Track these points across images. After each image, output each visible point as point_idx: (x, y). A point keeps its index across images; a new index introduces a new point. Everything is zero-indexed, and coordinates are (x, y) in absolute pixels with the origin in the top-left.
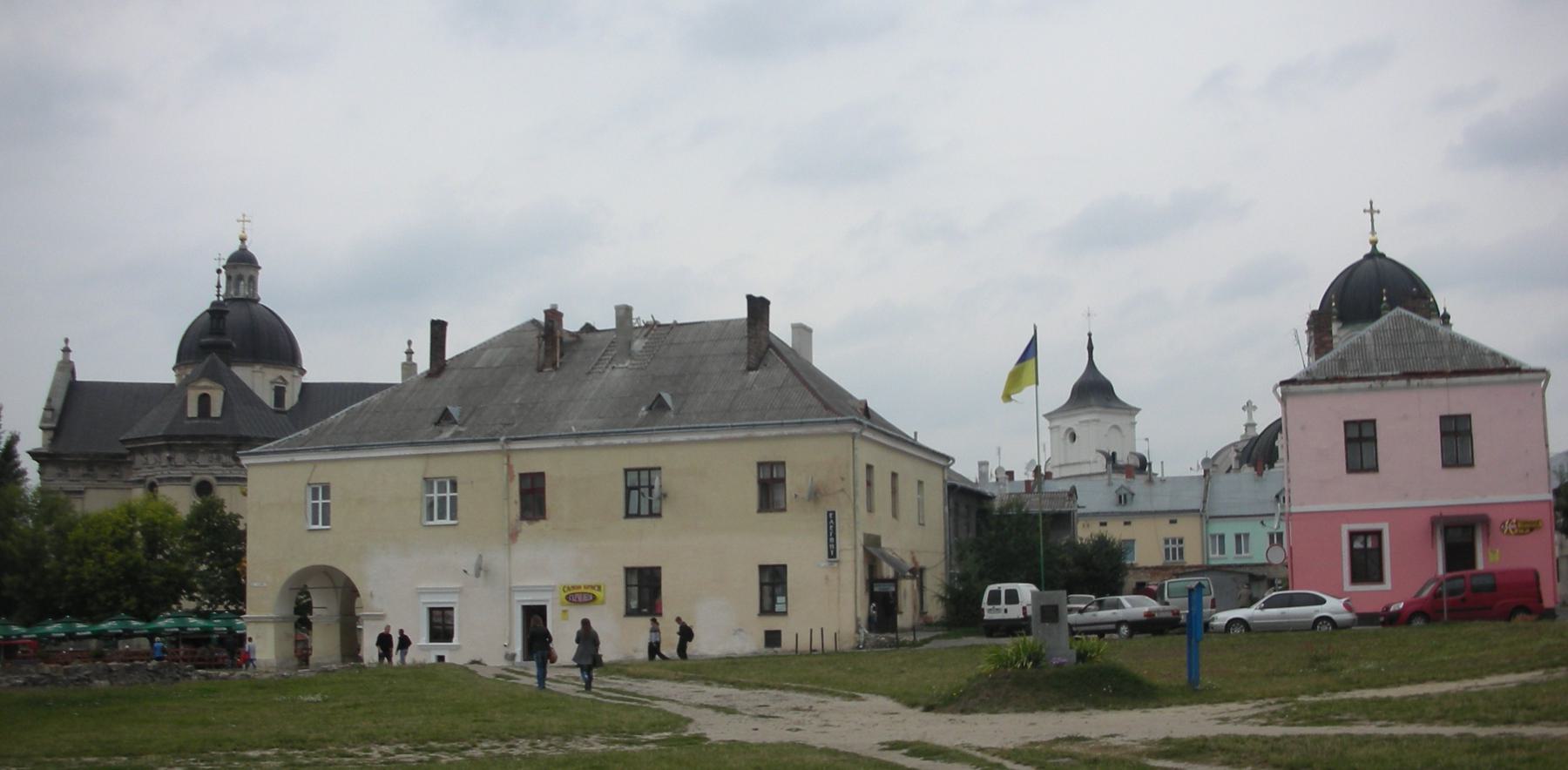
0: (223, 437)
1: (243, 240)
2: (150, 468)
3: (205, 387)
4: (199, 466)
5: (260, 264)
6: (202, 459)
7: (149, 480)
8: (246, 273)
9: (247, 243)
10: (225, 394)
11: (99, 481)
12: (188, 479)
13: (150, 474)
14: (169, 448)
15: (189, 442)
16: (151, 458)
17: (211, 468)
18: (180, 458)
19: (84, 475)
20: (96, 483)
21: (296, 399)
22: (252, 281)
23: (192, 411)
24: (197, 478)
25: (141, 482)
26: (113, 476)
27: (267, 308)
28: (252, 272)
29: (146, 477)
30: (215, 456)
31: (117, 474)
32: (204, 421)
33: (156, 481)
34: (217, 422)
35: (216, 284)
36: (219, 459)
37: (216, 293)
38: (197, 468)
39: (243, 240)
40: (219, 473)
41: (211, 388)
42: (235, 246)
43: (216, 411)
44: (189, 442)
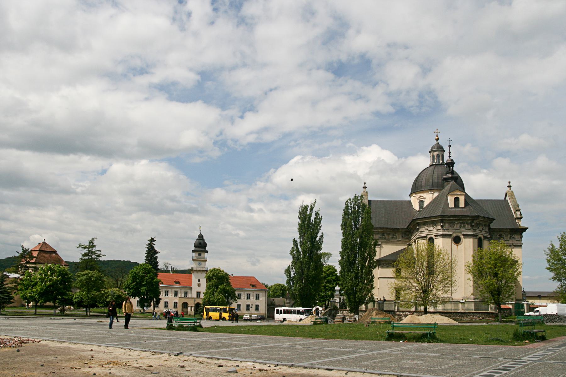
2: (429, 231)
4: (456, 229)
6: (457, 226)
11: (387, 240)
12: (450, 235)
14: (442, 221)
15: (452, 218)
17: (460, 230)
18: (447, 226)
19: (380, 238)
20: (385, 241)
23: (451, 205)
24: (454, 235)
25: (425, 237)
26: (393, 238)
31: (395, 237)
33: (433, 236)
35: (449, 152)
36: (464, 226)
38: (454, 230)
40: (465, 233)
44: (452, 218)
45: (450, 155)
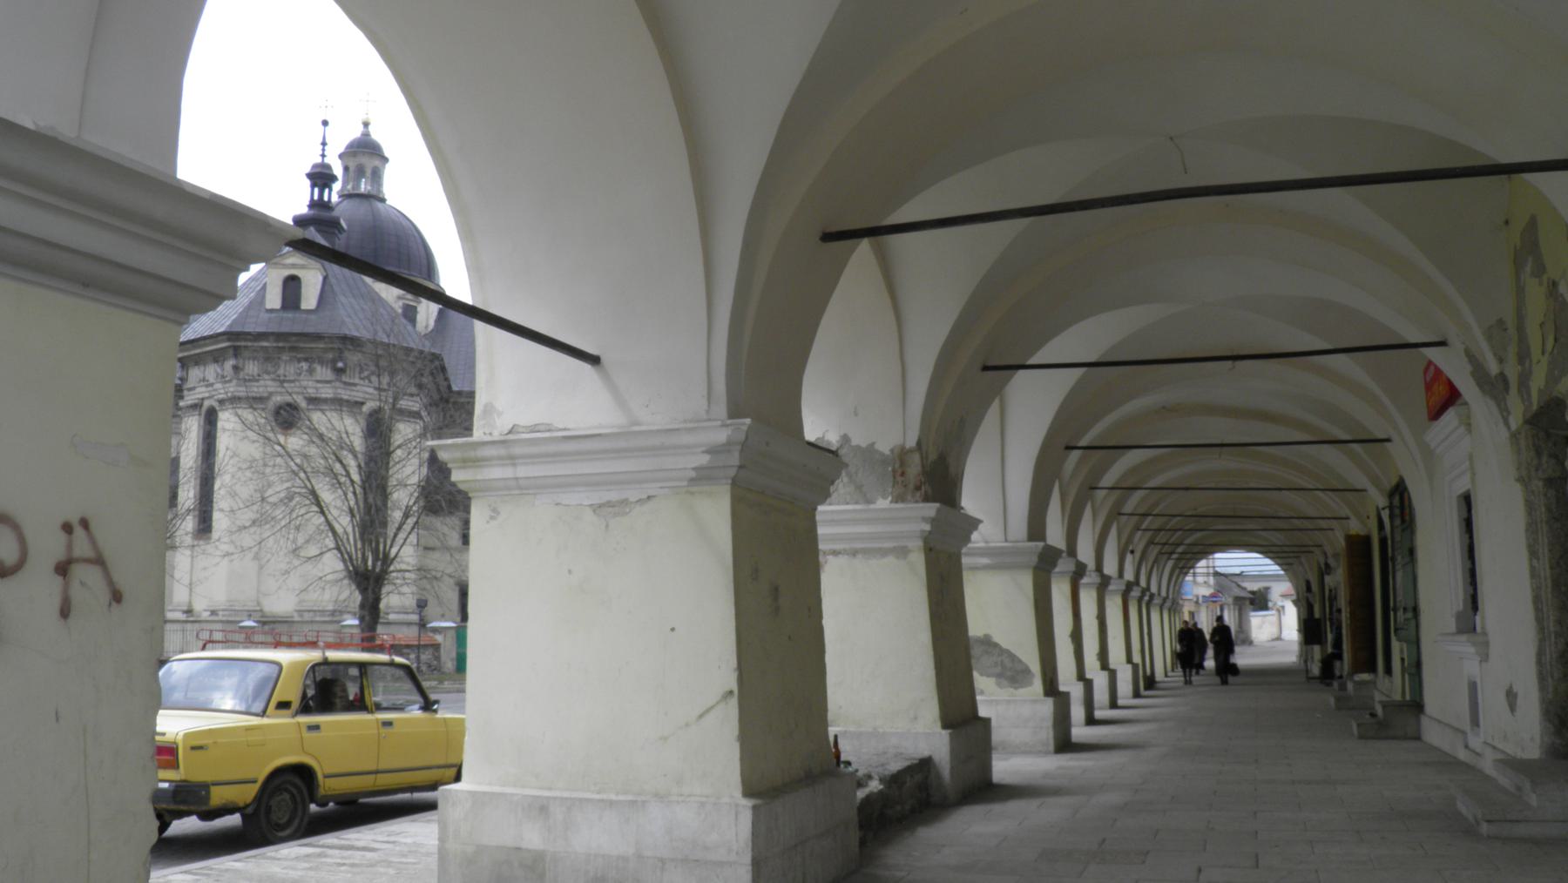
0: (318, 337)
1: (366, 124)
3: (294, 266)
5: (387, 154)
7: (207, 404)
8: (370, 163)
9: (371, 128)
10: (325, 279)
12: (261, 399)
13: (207, 395)
14: (237, 352)
16: (211, 371)
21: (432, 323)
22: (376, 176)
27: (398, 211)
28: (377, 163)
29: (203, 399)
30: (305, 365)
32: (290, 315)
33: (216, 404)
34: (313, 317)
35: (321, 140)
36: (311, 371)
37: (321, 153)
39: (366, 124)
41: (303, 267)
42: (356, 132)
43: (309, 300)
45: (323, 150)
